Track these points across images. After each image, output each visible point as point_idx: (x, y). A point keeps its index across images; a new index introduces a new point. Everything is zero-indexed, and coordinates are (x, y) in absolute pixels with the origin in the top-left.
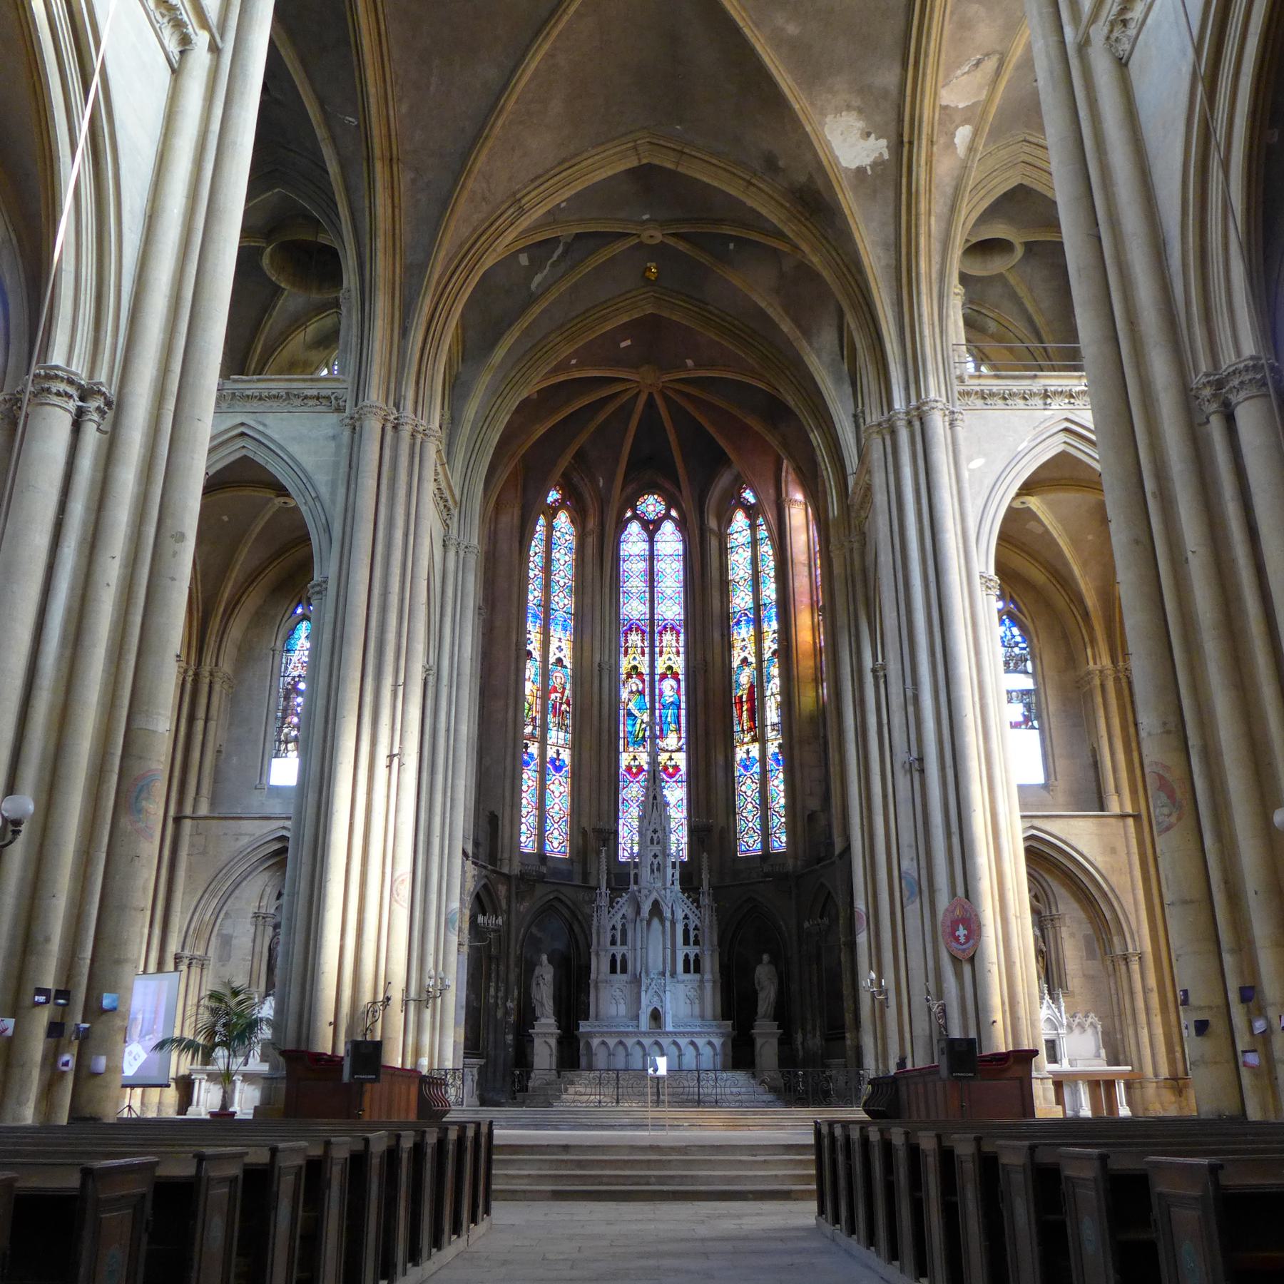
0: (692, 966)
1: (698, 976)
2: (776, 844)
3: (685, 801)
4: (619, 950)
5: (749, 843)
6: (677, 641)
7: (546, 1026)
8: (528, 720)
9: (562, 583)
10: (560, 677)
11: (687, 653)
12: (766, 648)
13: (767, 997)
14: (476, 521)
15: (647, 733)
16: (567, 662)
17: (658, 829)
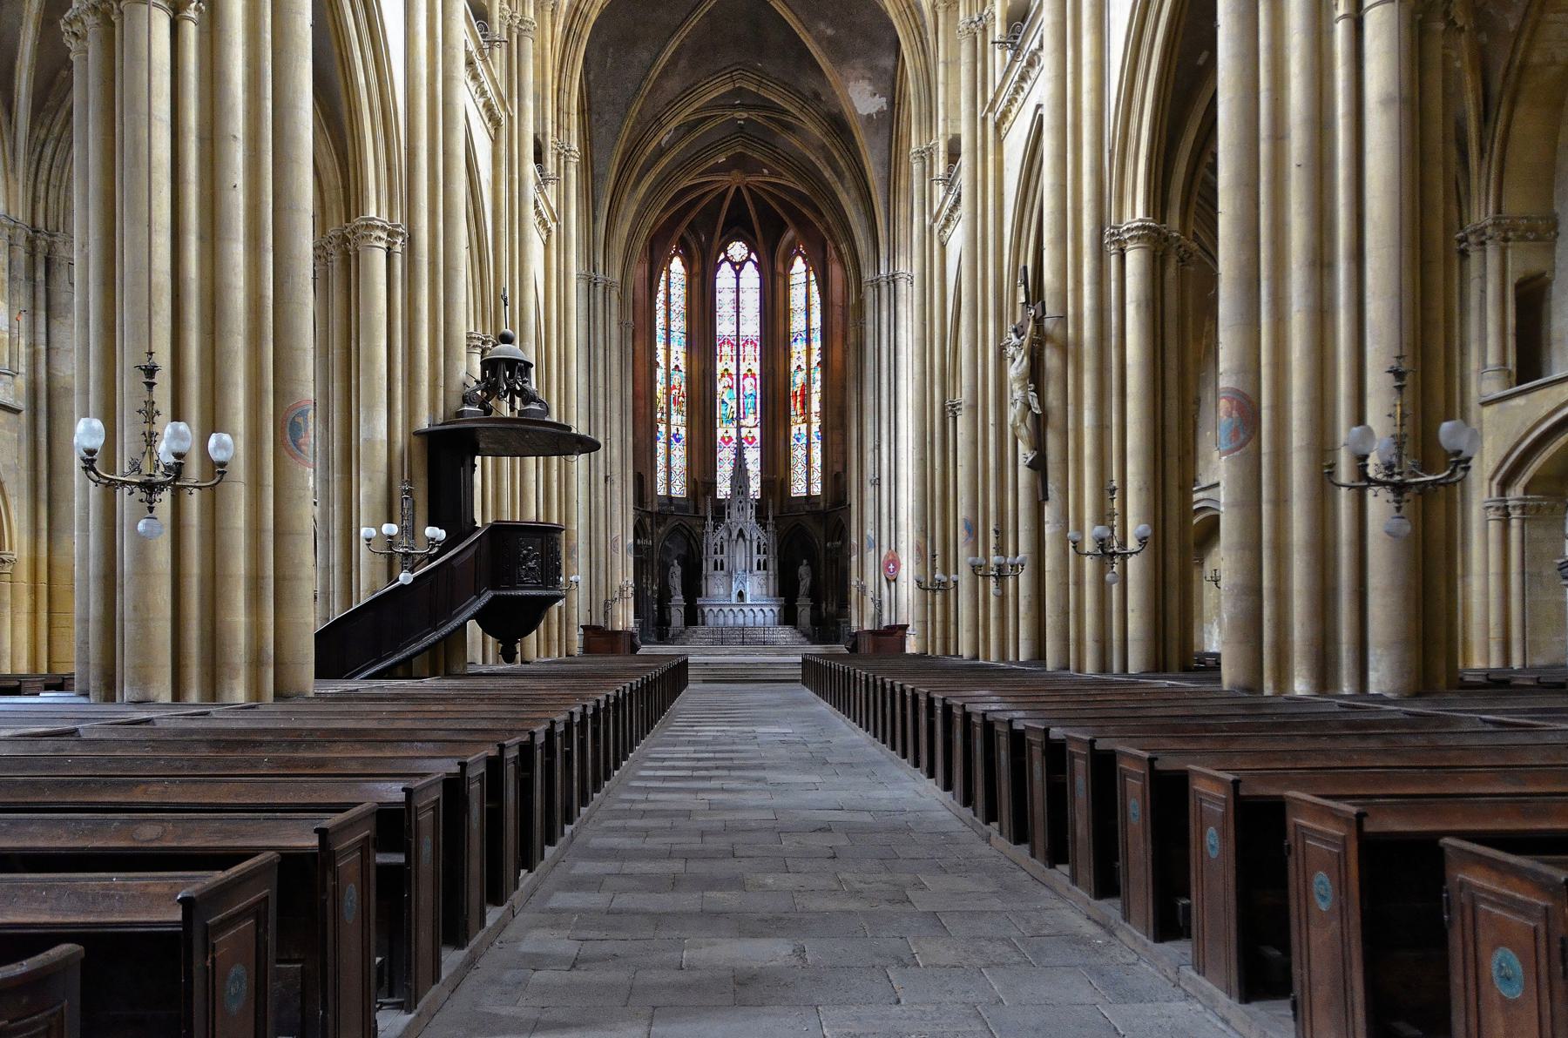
0: (762, 566)
1: (765, 572)
4: (719, 557)
5: (798, 489)
7: (678, 599)
10: (678, 379)
13: (805, 583)
15: (735, 416)
16: (682, 367)
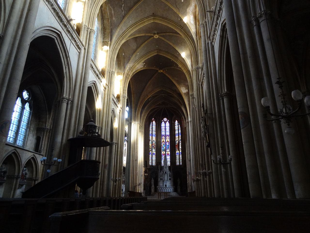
0: (170, 179)
10: (154, 143)
13: (179, 183)
16: (155, 141)
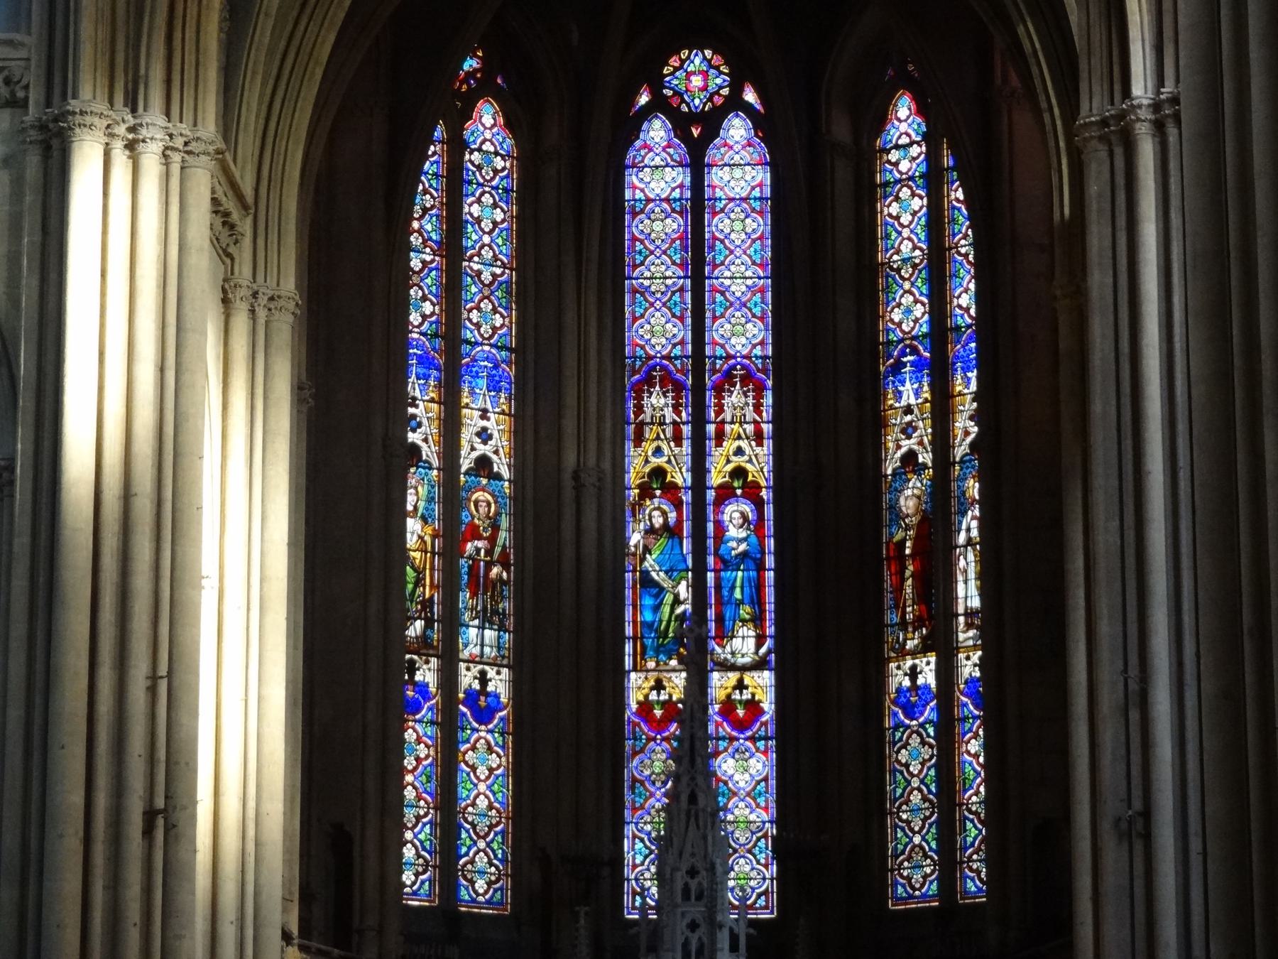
2: (971, 886)
3: (772, 783)
6: (758, 408)
8: (414, 608)
9: (487, 277)
11: (776, 436)
12: (959, 433)
14: (291, 240)
16: (502, 466)
17: (700, 865)
